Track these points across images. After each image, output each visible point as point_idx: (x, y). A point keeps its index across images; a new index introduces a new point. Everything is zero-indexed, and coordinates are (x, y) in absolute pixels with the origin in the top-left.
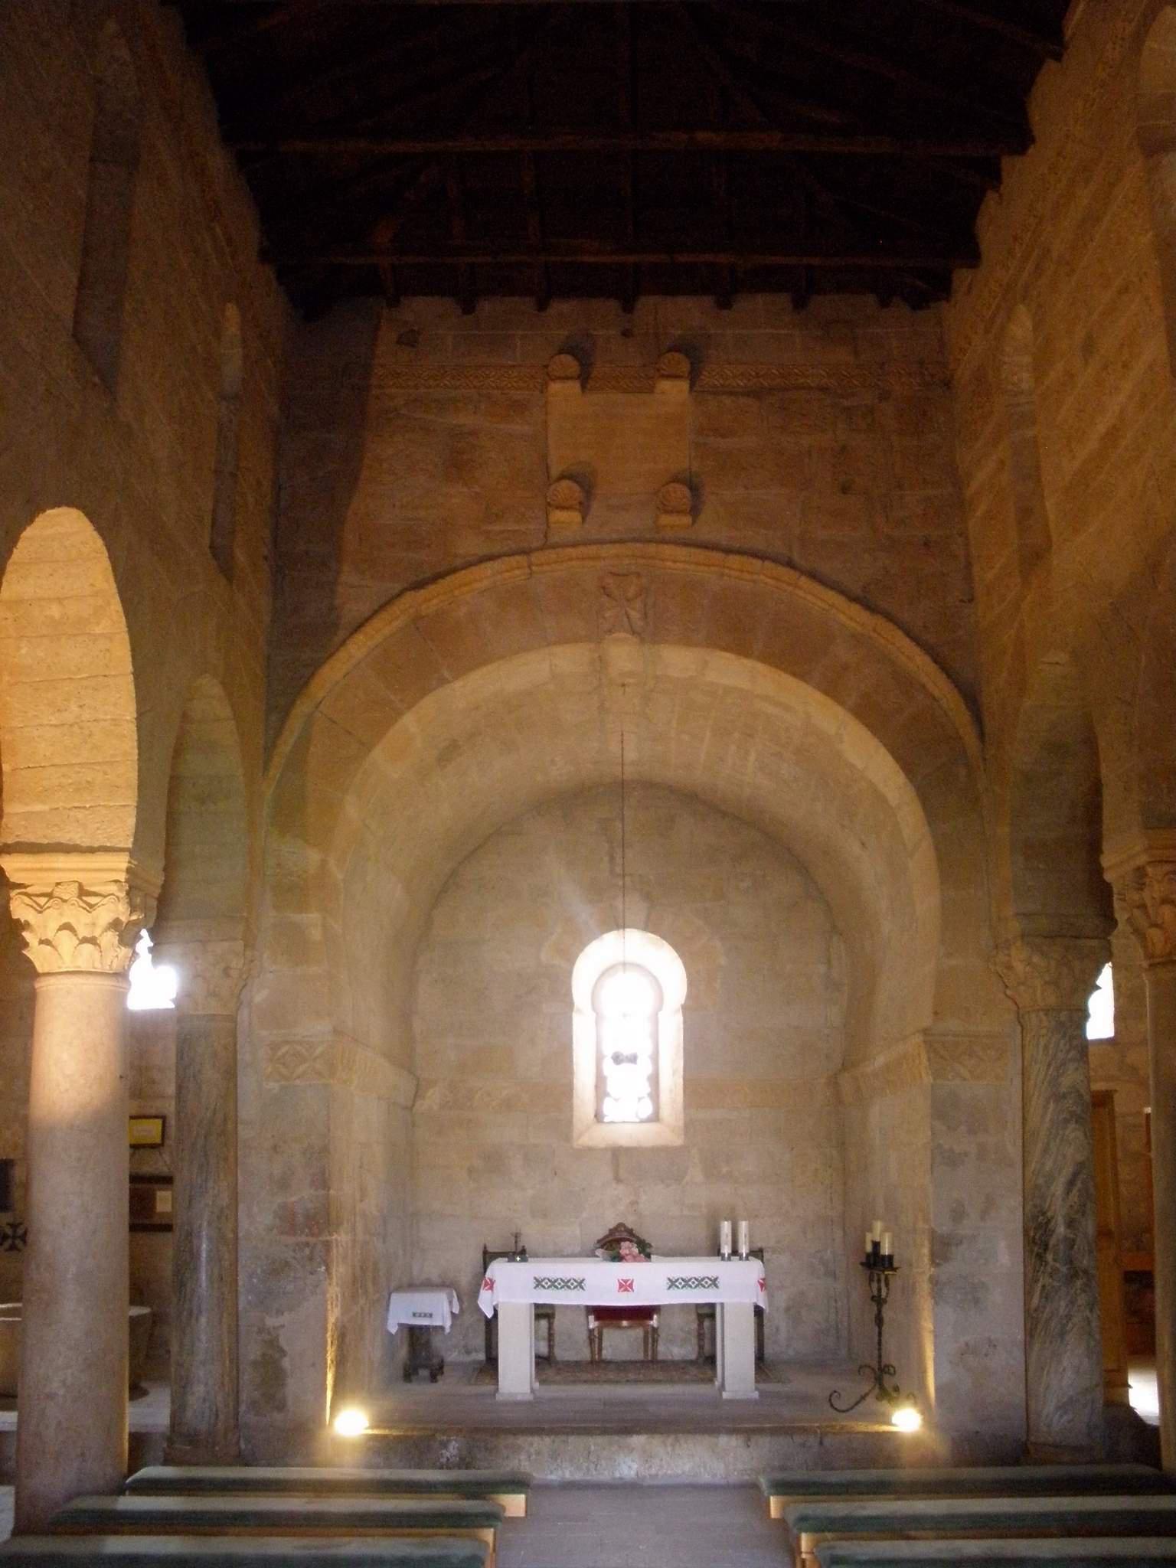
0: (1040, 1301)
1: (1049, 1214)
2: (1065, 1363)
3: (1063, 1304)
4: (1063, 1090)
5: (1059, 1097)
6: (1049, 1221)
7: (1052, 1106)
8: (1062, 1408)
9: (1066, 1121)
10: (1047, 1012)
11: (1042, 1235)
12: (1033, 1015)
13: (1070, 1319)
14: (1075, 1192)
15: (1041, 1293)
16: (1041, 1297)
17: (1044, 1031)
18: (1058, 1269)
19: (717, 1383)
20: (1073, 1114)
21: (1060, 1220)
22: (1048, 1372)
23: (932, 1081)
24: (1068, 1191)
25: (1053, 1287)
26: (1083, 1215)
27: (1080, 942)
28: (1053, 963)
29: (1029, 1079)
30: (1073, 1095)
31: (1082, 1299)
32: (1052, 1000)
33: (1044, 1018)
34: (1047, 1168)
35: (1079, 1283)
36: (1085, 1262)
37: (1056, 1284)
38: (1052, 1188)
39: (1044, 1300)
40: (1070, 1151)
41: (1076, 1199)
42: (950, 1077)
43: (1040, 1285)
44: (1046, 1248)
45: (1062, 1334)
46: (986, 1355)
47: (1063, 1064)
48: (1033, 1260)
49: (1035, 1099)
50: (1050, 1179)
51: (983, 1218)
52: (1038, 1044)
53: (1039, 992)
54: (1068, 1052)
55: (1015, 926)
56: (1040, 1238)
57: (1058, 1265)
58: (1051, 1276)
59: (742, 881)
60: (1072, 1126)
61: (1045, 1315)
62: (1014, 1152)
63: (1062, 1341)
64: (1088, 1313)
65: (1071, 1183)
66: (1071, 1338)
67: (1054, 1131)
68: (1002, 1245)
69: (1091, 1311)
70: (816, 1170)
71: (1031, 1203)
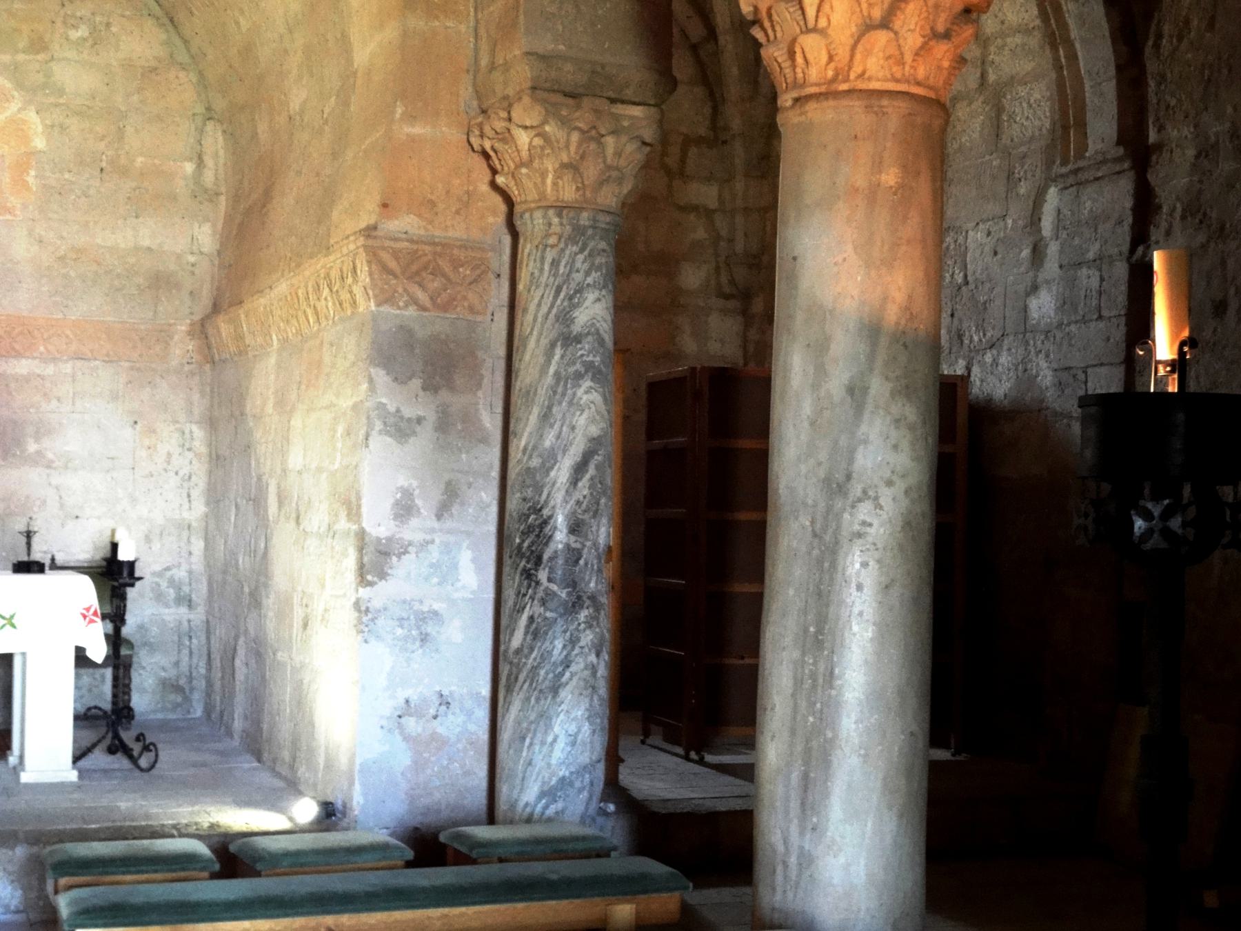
0: (524, 639)
1: (546, 512)
2: (557, 729)
3: (559, 644)
4: (576, 328)
5: (569, 340)
6: (545, 522)
7: (558, 352)
8: (549, 794)
9: (579, 376)
10: (560, 209)
11: (533, 543)
12: (538, 214)
13: (568, 667)
14: (584, 483)
15: (528, 627)
16: (526, 633)
17: (552, 240)
18: (555, 594)
19: (13, 760)
20: (589, 366)
21: (560, 520)
22: (531, 744)
23: (373, 308)
24: (574, 481)
25: (546, 618)
26: (594, 516)
27: (620, 109)
28: (575, 137)
29: (525, 310)
30: (590, 338)
31: (587, 638)
32: (569, 193)
33: (556, 220)
34: (547, 444)
35: (583, 615)
36: (592, 585)
37: (549, 614)
38: (553, 474)
39: (529, 637)
40: (581, 420)
41: (586, 492)
42: (401, 304)
43: (523, 620)
44: (538, 561)
45: (555, 690)
46: (435, 717)
47: (579, 290)
48: (517, 578)
49: (532, 344)
50: (551, 459)
51: (439, 517)
52: (543, 259)
53: (549, 181)
54: (587, 274)
55: (523, 73)
56: (529, 547)
57: (554, 587)
58: (543, 602)
59: (75, 27)
60: (587, 383)
61: (531, 661)
62: (491, 422)
63: (554, 697)
64: (592, 658)
65: (579, 469)
66: (566, 694)
67: (560, 390)
68: (465, 557)
69: (598, 655)
70: (169, 455)
71: (518, 495)
